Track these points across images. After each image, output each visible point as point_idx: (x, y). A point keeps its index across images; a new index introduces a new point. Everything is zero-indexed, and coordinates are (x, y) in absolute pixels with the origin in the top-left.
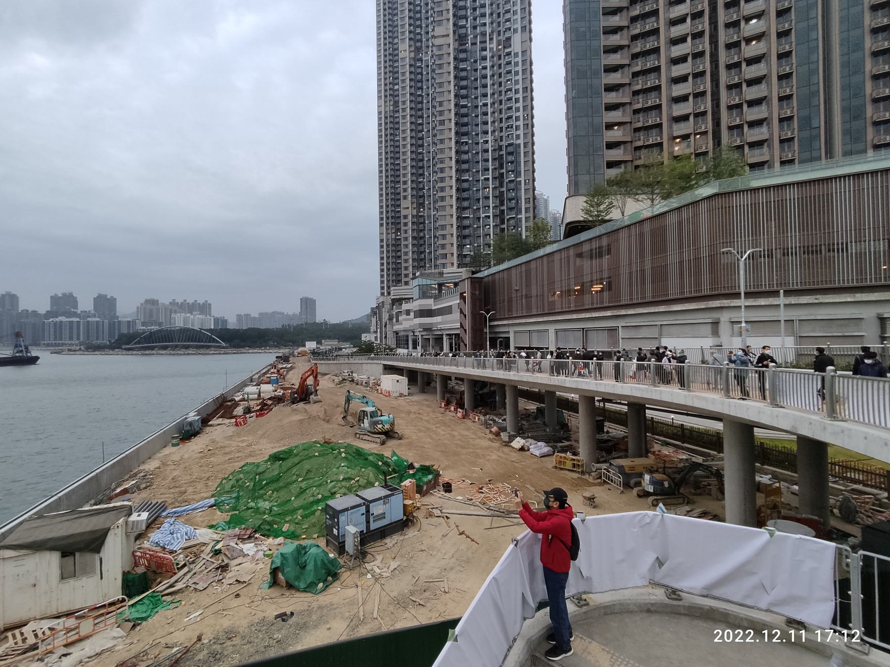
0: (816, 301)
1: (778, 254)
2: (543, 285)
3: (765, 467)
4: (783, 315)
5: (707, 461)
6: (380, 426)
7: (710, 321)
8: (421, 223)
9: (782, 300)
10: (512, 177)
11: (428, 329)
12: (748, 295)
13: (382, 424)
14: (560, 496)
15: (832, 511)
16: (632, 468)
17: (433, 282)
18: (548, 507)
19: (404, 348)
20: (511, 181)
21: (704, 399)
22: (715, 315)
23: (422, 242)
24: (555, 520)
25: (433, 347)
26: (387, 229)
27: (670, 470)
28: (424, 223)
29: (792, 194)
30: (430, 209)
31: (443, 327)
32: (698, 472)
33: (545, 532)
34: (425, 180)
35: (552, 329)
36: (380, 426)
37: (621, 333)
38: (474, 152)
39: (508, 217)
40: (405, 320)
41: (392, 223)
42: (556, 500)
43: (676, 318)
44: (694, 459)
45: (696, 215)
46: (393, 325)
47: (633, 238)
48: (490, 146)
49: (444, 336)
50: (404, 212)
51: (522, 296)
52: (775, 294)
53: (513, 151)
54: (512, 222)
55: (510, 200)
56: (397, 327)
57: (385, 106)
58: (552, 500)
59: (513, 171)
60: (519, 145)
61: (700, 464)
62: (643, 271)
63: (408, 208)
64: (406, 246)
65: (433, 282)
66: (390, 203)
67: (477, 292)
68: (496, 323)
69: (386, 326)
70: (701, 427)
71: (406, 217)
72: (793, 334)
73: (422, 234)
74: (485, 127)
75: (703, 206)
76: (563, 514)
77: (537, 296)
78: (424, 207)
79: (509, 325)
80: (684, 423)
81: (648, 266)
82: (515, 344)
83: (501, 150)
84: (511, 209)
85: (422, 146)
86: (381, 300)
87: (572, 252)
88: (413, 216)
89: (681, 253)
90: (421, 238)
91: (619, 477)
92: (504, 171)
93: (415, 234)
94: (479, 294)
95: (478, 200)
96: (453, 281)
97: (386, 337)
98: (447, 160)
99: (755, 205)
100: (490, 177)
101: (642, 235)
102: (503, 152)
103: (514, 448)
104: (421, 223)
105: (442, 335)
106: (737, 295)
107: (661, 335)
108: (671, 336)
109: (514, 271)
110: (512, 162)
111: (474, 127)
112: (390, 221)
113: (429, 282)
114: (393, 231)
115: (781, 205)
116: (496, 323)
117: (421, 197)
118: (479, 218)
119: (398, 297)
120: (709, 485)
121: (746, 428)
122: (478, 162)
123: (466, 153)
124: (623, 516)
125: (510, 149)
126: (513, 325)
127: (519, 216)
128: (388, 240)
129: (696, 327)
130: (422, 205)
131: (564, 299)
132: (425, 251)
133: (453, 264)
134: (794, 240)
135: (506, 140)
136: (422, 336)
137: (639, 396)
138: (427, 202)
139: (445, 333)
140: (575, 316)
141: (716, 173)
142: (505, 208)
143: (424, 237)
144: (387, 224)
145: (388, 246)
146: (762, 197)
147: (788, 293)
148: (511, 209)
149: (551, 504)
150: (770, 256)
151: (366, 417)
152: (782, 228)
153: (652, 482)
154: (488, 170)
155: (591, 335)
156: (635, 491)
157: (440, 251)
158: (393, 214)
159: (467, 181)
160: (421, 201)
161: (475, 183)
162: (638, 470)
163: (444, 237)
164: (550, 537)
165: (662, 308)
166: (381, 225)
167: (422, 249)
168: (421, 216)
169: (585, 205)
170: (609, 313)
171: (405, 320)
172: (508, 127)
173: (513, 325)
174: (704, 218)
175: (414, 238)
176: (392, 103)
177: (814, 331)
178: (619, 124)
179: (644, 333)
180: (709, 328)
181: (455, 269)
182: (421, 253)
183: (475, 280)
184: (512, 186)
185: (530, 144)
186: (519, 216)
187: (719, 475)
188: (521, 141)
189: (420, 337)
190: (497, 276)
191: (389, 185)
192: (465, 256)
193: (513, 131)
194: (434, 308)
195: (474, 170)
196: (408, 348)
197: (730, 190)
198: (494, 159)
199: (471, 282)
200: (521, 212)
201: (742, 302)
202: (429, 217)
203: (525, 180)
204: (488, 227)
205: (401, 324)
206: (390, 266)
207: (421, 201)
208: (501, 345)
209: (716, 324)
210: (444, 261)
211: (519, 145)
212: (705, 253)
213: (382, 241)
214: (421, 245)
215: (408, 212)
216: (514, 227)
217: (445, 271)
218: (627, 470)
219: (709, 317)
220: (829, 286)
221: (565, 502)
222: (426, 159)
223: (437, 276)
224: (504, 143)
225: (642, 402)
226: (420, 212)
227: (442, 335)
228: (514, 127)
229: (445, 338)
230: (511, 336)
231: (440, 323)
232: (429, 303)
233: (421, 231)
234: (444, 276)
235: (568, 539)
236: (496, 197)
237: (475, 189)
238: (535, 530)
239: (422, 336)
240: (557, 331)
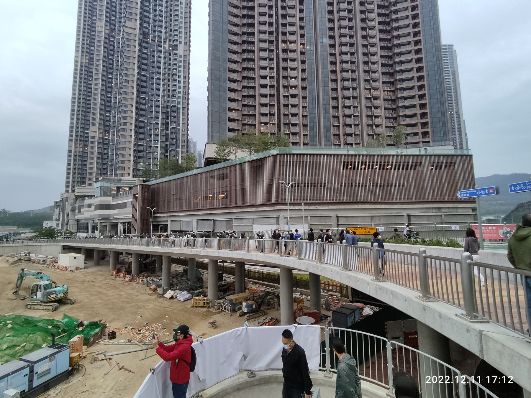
0: (316, 208)
1: (303, 185)
2: (190, 193)
3: (298, 289)
4: (303, 214)
5: (273, 290)
6: (54, 296)
7: (275, 216)
8: (106, 144)
9: (303, 207)
10: (174, 125)
11: (106, 218)
12: (291, 204)
13: (55, 293)
14: (184, 330)
15: (322, 306)
16: (237, 300)
17: (112, 185)
18: (176, 340)
19: (84, 232)
20: (173, 128)
21: (271, 257)
22: (278, 213)
23: (105, 157)
24: (181, 348)
25: (109, 231)
26: (76, 144)
27: (256, 298)
28: (108, 144)
29: (307, 159)
30: (114, 135)
31: (118, 217)
32: (269, 297)
33: (173, 359)
34: (111, 116)
35: (195, 219)
36: (54, 296)
37: (234, 222)
38: (149, 105)
39: (170, 149)
40: (86, 211)
41: (81, 140)
42: (181, 333)
43: (260, 214)
44: (268, 290)
45: (270, 163)
46: (75, 215)
47: (241, 171)
48: (160, 104)
49: (119, 224)
50: (91, 134)
51: (177, 198)
52: (300, 204)
53: (176, 110)
54: (173, 152)
55: (172, 139)
56: (78, 217)
57: (82, 58)
58: (179, 334)
59: (175, 122)
60: (180, 108)
61: (270, 292)
63: (96, 132)
64: (92, 158)
65: (112, 185)
66: (80, 125)
67: (146, 195)
68: (158, 215)
69: (68, 215)
70: (271, 272)
71: (93, 138)
72: (308, 223)
73: (106, 151)
74: (158, 92)
75: (273, 159)
76: (187, 342)
77: (187, 199)
78: (109, 133)
79: (167, 217)
80: (264, 271)
81: (248, 186)
82: (171, 228)
83: (168, 108)
84: (173, 145)
85: (111, 92)
86: (65, 195)
87: (208, 175)
88: (99, 138)
89: (263, 181)
90: (105, 154)
91: (230, 307)
92: (169, 121)
93: (100, 151)
94: (148, 196)
95: (151, 135)
96: (128, 186)
97: (67, 224)
98: (129, 106)
99: (294, 162)
100: (160, 123)
101: (245, 169)
102: (169, 110)
103: (166, 298)
104: (106, 144)
105: (118, 223)
106: (285, 204)
107: (253, 223)
108: (258, 224)
109: (172, 182)
110: (174, 117)
111: (150, 90)
112: (79, 138)
113: (109, 185)
114: (81, 146)
115: (303, 162)
116: (158, 215)
117: (107, 126)
118: (150, 147)
119: (82, 194)
120: (274, 303)
121: (289, 271)
122: (152, 112)
123: (144, 104)
124: (226, 334)
125: (174, 109)
126: (170, 216)
127: (177, 150)
128: (75, 152)
129: (269, 219)
130: (108, 132)
131: (203, 202)
132: (108, 164)
133: (129, 174)
134: (308, 180)
135: (171, 103)
136: (101, 223)
137: (241, 258)
138: (111, 130)
139: (120, 221)
140: (209, 212)
141: (279, 144)
142: (168, 143)
143: (108, 153)
144: (76, 140)
145: (75, 156)
146: (296, 158)
147: (306, 204)
148: (173, 145)
149: (178, 337)
150: (299, 186)
151: (39, 290)
152: (304, 174)
153: (247, 306)
154: (159, 118)
155: (217, 223)
156: (238, 312)
157: (120, 165)
158: (82, 134)
159: (143, 122)
160: (107, 128)
161: (149, 124)
162: (240, 300)
163: (123, 155)
164: (177, 360)
165: (254, 209)
166: (71, 140)
167: (105, 162)
168: (106, 139)
169: (216, 149)
170: (227, 211)
171: (86, 211)
172: (173, 96)
173: (170, 216)
174: (273, 165)
175: (99, 153)
176: (88, 58)
177: (315, 222)
178: (236, 110)
180: (275, 220)
181: (131, 177)
182: (105, 164)
183: (144, 186)
184: (174, 131)
185: (186, 108)
186: (177, 150)
187: (278, 297)
188: (181, 106)
189: (99, 224)
190: (161, 185)
191: (81, 113)
192: (139, 170)
193: (176, 99)
194: (112, 203)
195: (149, 117)
196: (87, 232)
197: (284, 153)
198: (163, 113)
199: (142, 188)
200: (179, 148)
201: (288, 207)
202: (113, 140)
203: (182, 129)
204: (157, 153)
205: (83, 214)
206: (77, 171)
207: (107, 128)
208: (161, 230)
209: (278, 218)
210: (122, 172)
211: (180, 108)
212: (273, 182)
213: (70, 152)
214: (105, 159)
215: (96, 135)
216: (174, 156)
217: (123, 178)
218: (234, 302)
219: (274, 214)
220: (320, 202)
221: (187, 333)
222: (113, 102)
223: (116, 181)
224: (170, 104)
225: (243, 261)
226: (106, 136)
227: (118, 223)
228: (177, 97)
229: (119, 225)
230: (169, 224)
231: (116, 214)
232: (108, 200)
233: (105, 149)
234: (122, 182)
235: (189, 359)
236: (163, 135)
237: (148, 128)
238: (166, 359)
240: (198, 221)
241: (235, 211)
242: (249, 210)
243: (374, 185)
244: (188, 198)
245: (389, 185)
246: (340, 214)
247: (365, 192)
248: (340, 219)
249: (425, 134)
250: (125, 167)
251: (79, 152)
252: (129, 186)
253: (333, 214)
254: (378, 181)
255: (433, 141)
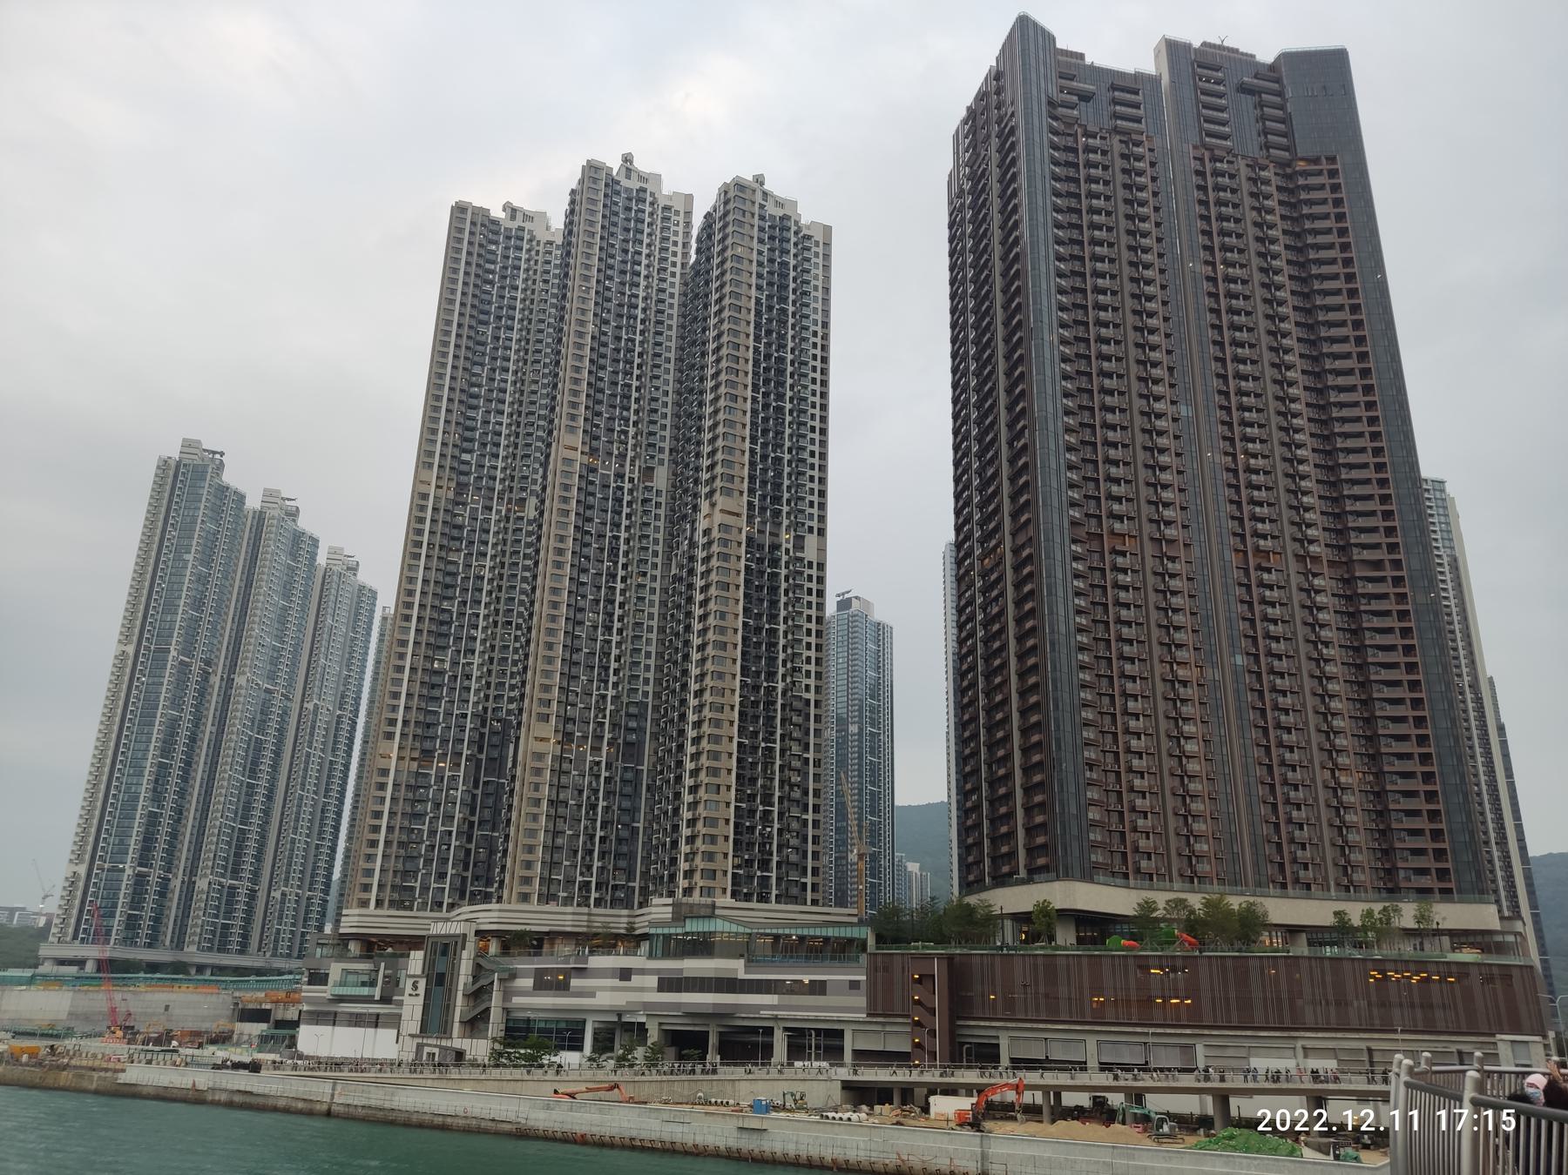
19: (572, 1048)
31: (781, 1014)
35: (1091, 1042)
46: (507, 995)
62: (1227, 999)
72: (1336, 1058)
77: (1070, 999)
81: (1232, 995)
89: (1264, 992)
96: (768, 931)
126: (1007, 1029)
131: (1120, 1010)
133: (724, 890)
165: (1249, 1033)
170: (1188, 1031)
173: (1007, 1029)
176: (453, 485)
179: (1230, 1052)
188: (811, 696)
194: (742, 975)
211: (808, 701)
230: (1004, 1044)
234: (718, 912)
239: (660, 1024)
241: (1206, 1032)
242: (1239, 1033)
243: (1412, 1006)
244: (1073, 996)
245: (1431, 1006)
246: (1374, 1045)
247: (1402, 1015)
248: (1375, 1054)
249: (1443, 874)
250: (715, 871)
251: (409, 772)
252: (774, 931)
253: (1363, 1045)
254: (1417, 1000)
255: (1460, 891)
